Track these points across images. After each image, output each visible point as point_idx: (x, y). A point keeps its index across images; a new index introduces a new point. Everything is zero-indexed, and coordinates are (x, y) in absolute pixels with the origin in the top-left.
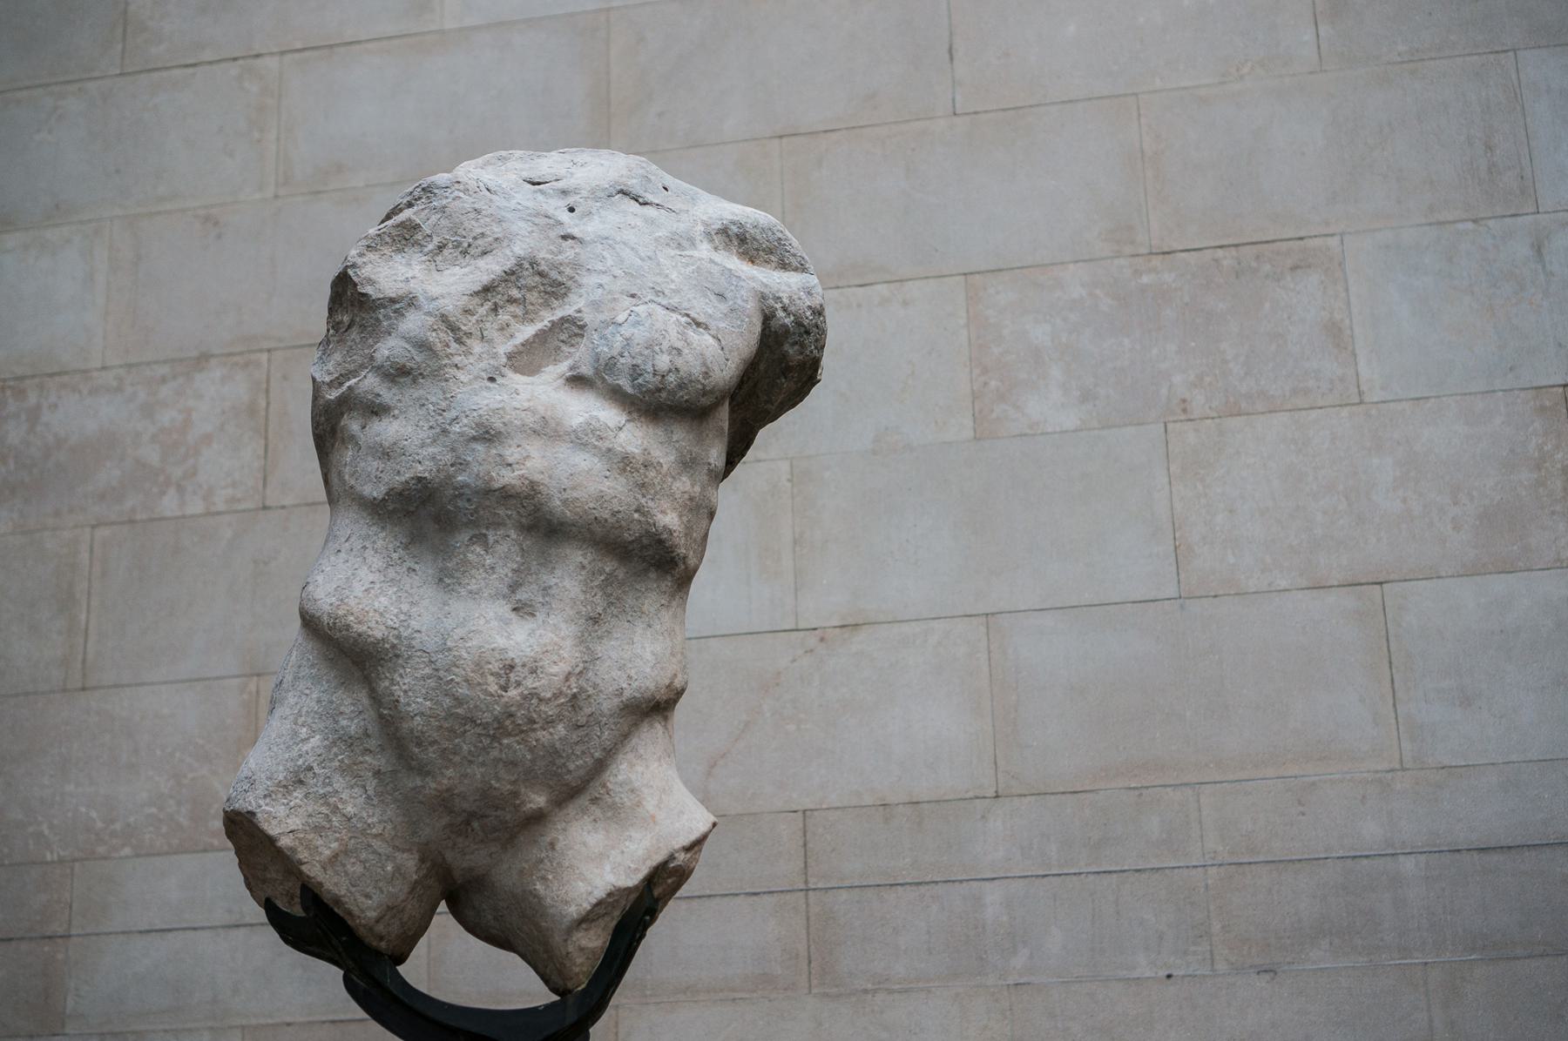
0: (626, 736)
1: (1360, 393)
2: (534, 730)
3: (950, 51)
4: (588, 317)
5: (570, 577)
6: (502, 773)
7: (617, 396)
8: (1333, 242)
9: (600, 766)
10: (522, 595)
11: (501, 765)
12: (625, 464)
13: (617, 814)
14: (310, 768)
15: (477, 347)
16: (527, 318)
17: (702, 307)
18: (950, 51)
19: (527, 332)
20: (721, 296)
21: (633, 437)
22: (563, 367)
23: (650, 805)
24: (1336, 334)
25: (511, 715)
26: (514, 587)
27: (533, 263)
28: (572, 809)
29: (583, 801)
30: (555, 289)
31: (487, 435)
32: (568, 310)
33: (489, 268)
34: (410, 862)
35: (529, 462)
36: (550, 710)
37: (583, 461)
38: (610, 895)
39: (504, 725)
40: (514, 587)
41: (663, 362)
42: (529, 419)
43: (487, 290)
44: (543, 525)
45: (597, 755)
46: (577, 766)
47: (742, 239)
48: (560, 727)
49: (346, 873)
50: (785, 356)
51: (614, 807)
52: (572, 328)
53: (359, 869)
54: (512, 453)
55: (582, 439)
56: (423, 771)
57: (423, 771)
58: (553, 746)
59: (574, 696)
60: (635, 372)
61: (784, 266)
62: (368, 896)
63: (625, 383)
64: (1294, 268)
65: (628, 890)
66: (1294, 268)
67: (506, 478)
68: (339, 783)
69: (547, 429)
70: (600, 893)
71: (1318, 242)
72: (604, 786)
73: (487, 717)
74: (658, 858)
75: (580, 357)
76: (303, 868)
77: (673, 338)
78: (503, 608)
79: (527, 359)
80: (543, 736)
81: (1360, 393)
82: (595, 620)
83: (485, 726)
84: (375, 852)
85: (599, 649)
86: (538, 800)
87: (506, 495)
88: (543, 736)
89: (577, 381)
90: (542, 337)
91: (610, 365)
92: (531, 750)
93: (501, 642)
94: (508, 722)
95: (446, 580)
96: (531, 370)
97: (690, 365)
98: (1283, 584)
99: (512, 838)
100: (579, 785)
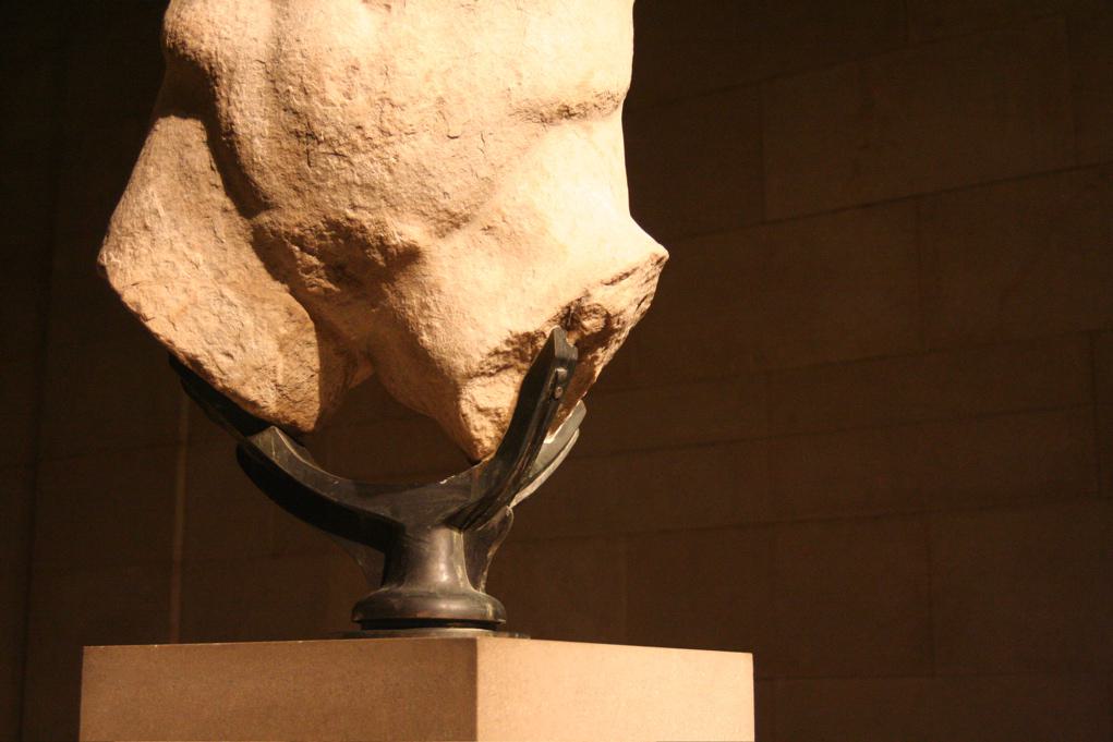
0: (525, 149)
2: (388, 144)
6: (360, 200)
11: (356, 190)
14: (156, 212)
25: (359, 127)
28: (459, 239)
38: (508, 342)
45: (483, 173)
48: (425, 138)
49: (201, 330)
51: (512, 236)
53: (212, 324)
58: (419, 163)
59: (441, 100)
62: (228, 355)
70: (497, 340)
72: (498, 211)
73: (331, 132)
74: (567, 297)
76: (149, 324)
83: (329, 142)
84: (231, 304)
88: (406, 151)
92: (390, 171)
94: (355, 136)
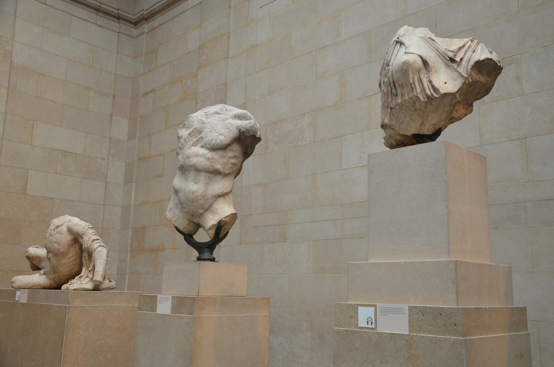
1: (523, 93)
3: (436, 25)
4: (204, 136)
5: (202, 177)
7: (207, 148)
8: (519, 56)
9: (211, 206)
10: (196, 181)
12: (208, 159)
13: (214, 213)
15: (188, 143)
16: (196, 137)
17: (222, 131)
18: (436, 25)
19: (195, 140)
20: (228, 129)
21: (209, 154)
22: (200, 145)
23: (219, 211)
24: (518, 79)
26: (194, 180)
27: (196, 129)
28: (208, 212)
29: (209, 211)
30: (200, 132)
31: (188, 157)
32: (201, 136)
33: (191, 130)
34: (186, 221)
35: (194, 161)
36: (200, 198)
37: (202, 159)
39: (193, 201)
40: (194, 180)
41: (214, 142)
42: (194, 154)
43: (190, 134)
44: (198, 170)
46: (206, 206)
47: (239, 117)
50: (246, 136)
52: (202, 138)
54: (191, 160)
55: (202, 156)
56: (184, 208)
57: (184, 208)
60: (209, 144)
61: (247, 120)
63: (208, 146)
64: (509, 64)
65: (215, 225)
66: (509, 64)
67: (191, 163)
68: (175, 210)
69: (197, 155)
70: (211, 225)
71: (515, 57)
74: (220, 219)
75: (202, 143)
77: (216, 138)
78: (193, 183)
79: (195, 144)
80: (199, 202)
81: (523, 93)
82: (207, 183)
85: (208, 188)
86: (201, 211)
87: (191, 166)
88: (199, 202)
89: (202, 147)
90: (197, 140)
91: (206, 144)
93: (192, 188)
95: (186, 179)
96: (196, 146)
97: (219, 142)
98: (503, 140)
99: (199, 217)
100: (208, 209)
